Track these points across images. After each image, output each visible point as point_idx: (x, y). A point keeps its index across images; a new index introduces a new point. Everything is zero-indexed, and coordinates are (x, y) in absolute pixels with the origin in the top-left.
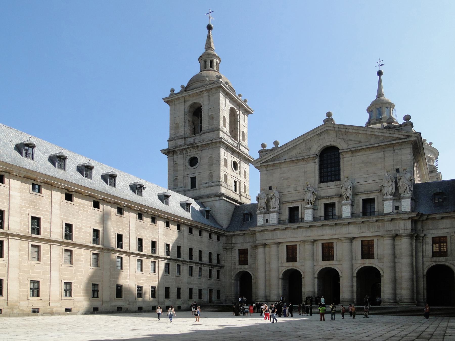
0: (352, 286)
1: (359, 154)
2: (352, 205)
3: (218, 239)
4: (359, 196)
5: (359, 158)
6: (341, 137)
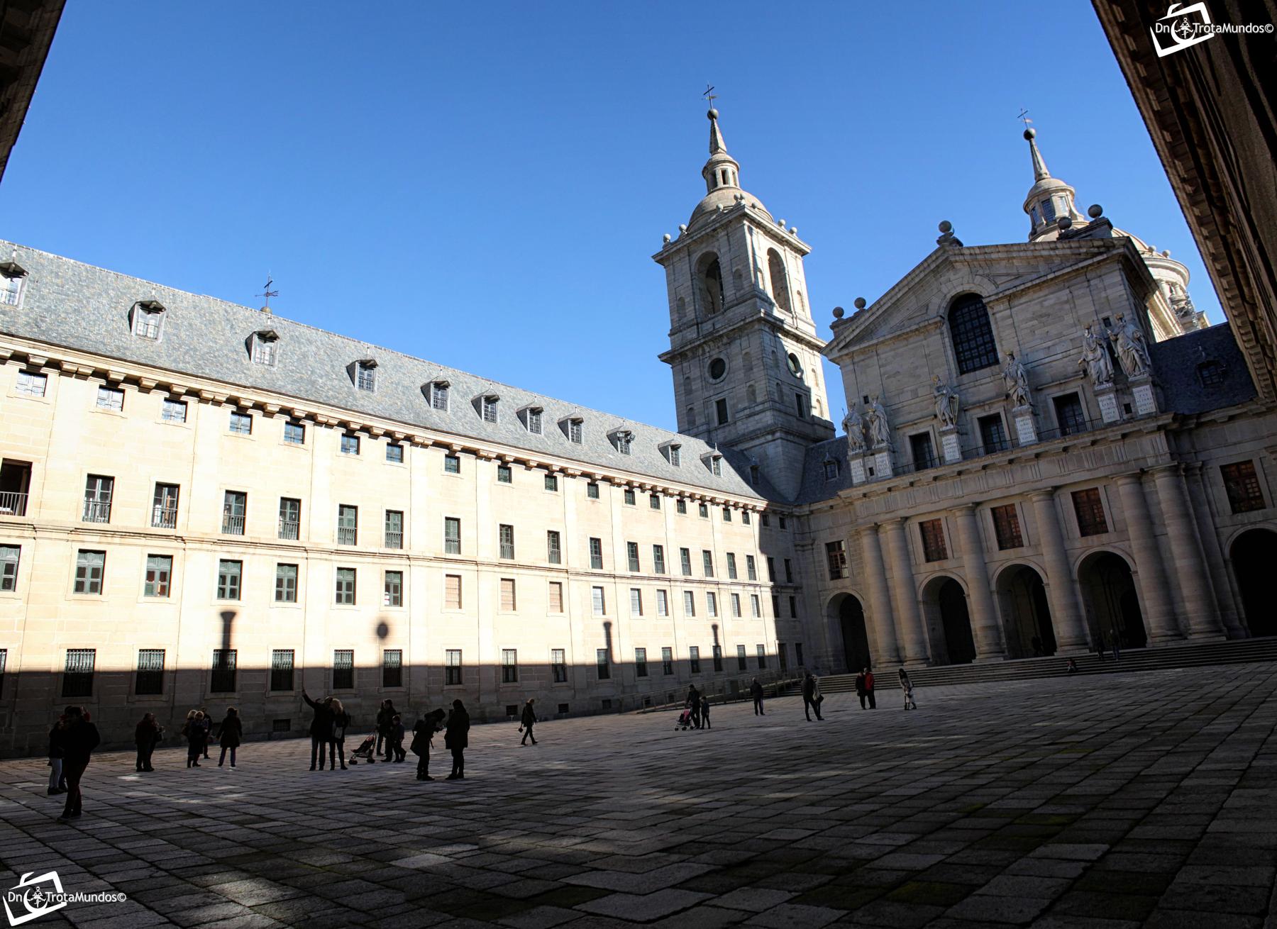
0: (1075, 606)
1: (1023, 300)
2: (1035, 414)
3: (783, 526)
4: (1046, 392)
5: (1025, 310)
6: (981, 272)
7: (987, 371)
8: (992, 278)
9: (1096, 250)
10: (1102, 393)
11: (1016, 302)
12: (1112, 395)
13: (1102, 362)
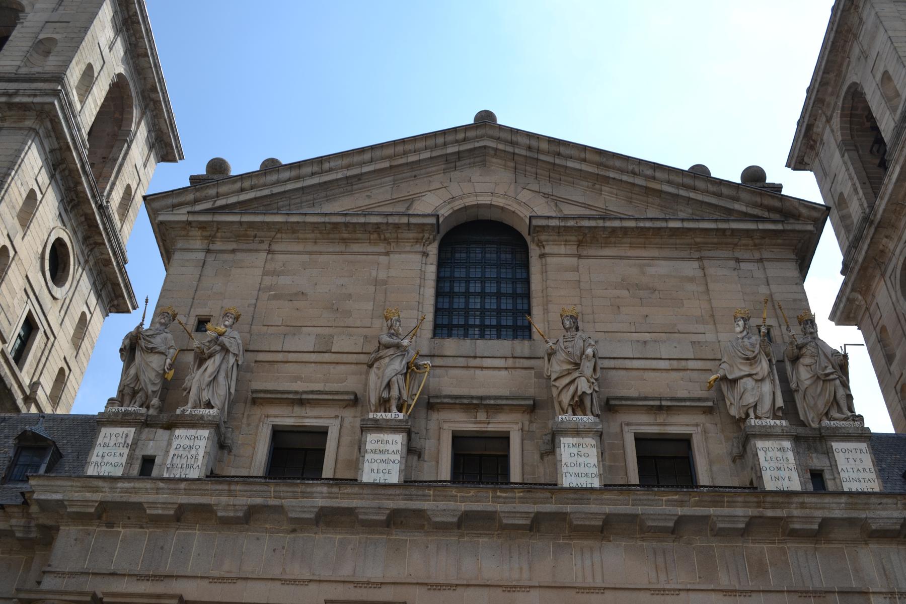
7: (504, 346)
8: (557, 201)
9: (766, 215)
10: (767, 434)
11: (592, 252)
12: (787, 444)
13: (767, 387)
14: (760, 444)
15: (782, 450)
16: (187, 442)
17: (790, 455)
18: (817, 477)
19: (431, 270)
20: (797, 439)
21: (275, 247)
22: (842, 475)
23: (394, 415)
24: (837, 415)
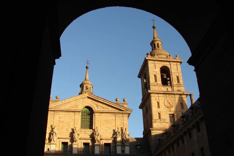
9: (124, 110)
10: (118, 145)
12: (120, 147)
14: (117, 147)
15: (120, 148)
16: (53, 147)
17: (120, 148)
18: (123, 151)
19: (80, 117)
20: (121, 146)
21: (60, 113)
22: (126, 151)
23: (77, 143)
24: (127, 143)
